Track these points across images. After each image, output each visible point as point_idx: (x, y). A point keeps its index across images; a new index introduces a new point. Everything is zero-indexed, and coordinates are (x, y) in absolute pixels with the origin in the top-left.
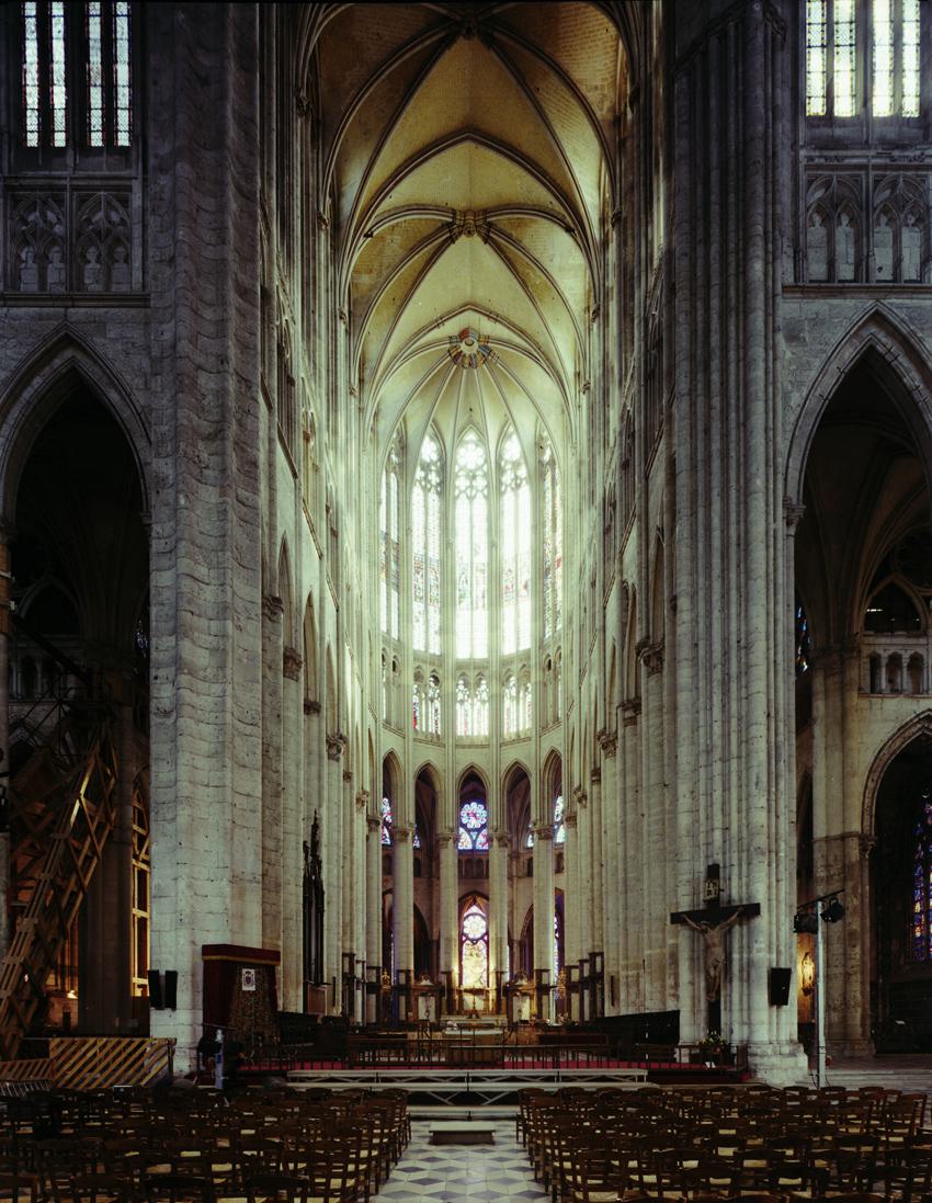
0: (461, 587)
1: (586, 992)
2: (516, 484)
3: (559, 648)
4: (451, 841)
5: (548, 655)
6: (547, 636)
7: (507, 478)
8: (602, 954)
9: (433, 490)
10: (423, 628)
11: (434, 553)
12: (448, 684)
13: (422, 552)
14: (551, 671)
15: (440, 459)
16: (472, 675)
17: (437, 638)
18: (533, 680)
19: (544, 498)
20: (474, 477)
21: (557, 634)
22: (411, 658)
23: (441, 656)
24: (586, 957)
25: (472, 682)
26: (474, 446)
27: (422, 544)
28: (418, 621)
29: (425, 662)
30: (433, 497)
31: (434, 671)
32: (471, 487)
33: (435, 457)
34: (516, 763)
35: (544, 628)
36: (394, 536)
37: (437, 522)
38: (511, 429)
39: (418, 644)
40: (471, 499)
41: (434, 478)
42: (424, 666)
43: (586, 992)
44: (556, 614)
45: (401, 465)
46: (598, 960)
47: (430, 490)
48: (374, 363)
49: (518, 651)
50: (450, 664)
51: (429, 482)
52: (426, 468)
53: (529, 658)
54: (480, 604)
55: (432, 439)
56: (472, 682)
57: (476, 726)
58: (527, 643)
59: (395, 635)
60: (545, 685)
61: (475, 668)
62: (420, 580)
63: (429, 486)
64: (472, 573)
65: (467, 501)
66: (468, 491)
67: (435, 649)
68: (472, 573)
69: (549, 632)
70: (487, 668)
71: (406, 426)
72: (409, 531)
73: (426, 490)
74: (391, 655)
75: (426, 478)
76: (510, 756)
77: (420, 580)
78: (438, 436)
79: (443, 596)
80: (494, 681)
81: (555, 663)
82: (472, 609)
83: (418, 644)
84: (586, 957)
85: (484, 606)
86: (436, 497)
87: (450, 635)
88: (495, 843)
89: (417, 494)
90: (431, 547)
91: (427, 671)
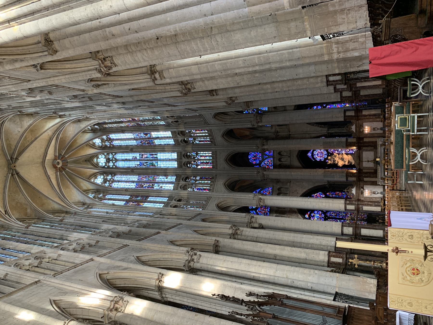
0: (149, 165)
1: (359, 85)
2: (109, 140)
3: (167, 117)
4: (265, 173)
5: (172, 122)
6: (164, 123)
7: (107, 144)
8: (327, 76)
9: (113, 178)
10: (164, 185)
11: (135, 178)
12: (189, 172)
13: (135, 184)
14: (179, 121)
15: (103, 174)
16: (185, 160)
17: (169, 177)
18: (184, 130)
19: (112, 127)
20: (109, 159)
21: (163, 119)
22: (176, 191)
23: (176, 176)
24: (331, 88)
25: (187, 160)
26: (99, 159)
27: (132, 184)
28: (162, 187)
29: (179, 184)
30: (117, 178)
31: (182, 180)
32: (112, 160)
33: (102, 177)
34: (223, 136)
35: (161, 125)
36: (127, 197)
37: (125, 176)
38: (91, 142)
39: (170, 187)
40: (116, 160)
41: (109, 177)
42: (180, 185)
43: (359, 85)
44: (154, 120)
45: (103, 193)
46: (331, 78)
47: (113, 179)
48: (61, 207)
49: (172, 138)
50: (179, 172)
51: (110, 179)
52: (105, 181)
53: (175, 132)
54: (155, 156)
55: (96, 178)
56: (187, 160)
57: (208, 158)
58: (169, 134)
59: (165, 200)
60: (185, 123)
61: (181, 159)
62: (146, 185)
63: (112, 180)
64: (143, 160)
65: (117, 163)
66: (114, 162)
67: (173, 179)
68: (143, 160)
69: (162, 123)
70: (181, 153)
71: (91, 190)
72: (127, 190)
73: (114, 181)
74: (174, 203)
75: (109, 181)
76: (219, 139)
77: (146, 185)
78: (95, 175)
79: (152, 174)
80: (186, 149)
81: (174, 119)
82: (157, 160)
83: (170, 187)
84: (331, 88)
85: (156, 155)
86: (116, 177)
87: (168, 171)
88: (265, 147)
89: (115, 185)
90: (134, 179)
91: (182, 183)
